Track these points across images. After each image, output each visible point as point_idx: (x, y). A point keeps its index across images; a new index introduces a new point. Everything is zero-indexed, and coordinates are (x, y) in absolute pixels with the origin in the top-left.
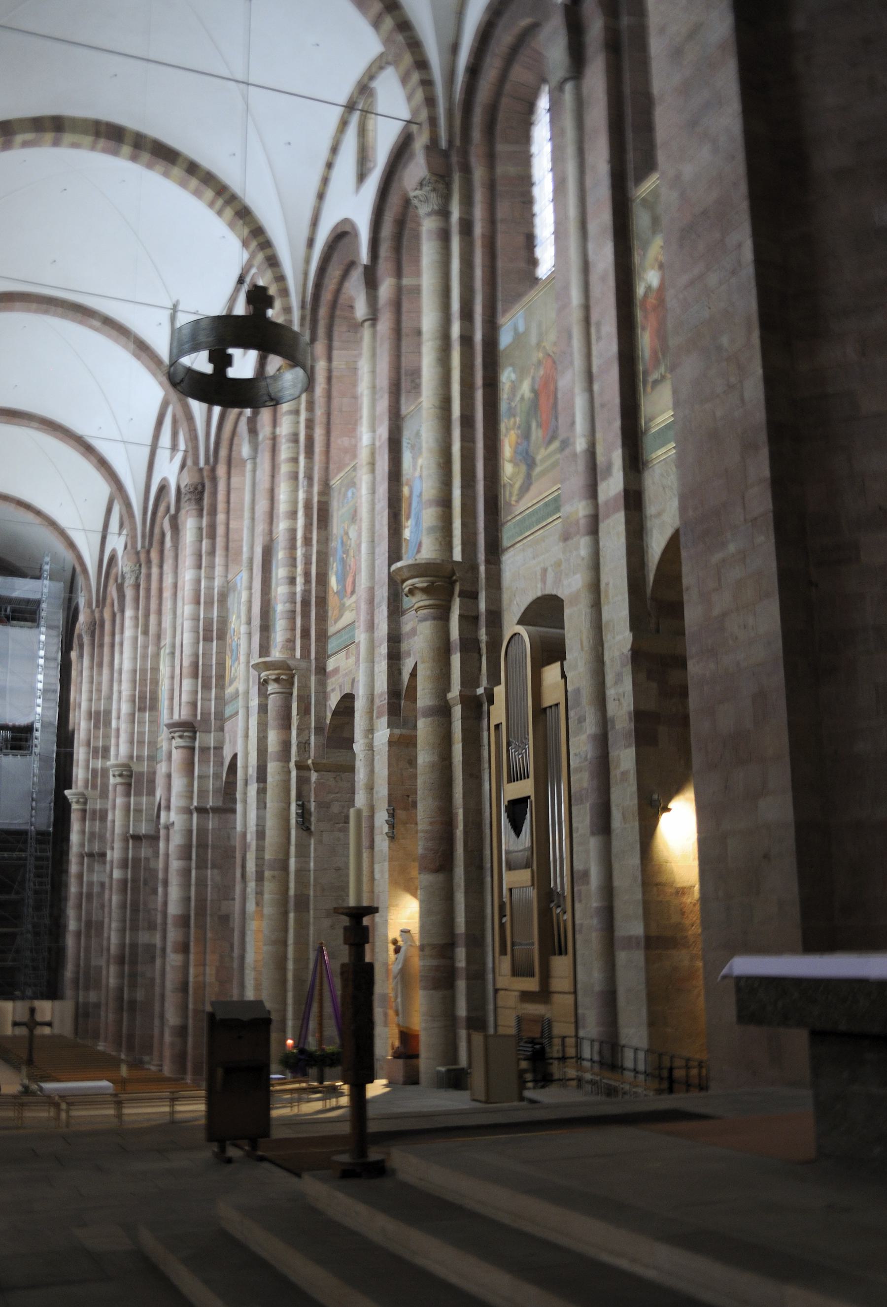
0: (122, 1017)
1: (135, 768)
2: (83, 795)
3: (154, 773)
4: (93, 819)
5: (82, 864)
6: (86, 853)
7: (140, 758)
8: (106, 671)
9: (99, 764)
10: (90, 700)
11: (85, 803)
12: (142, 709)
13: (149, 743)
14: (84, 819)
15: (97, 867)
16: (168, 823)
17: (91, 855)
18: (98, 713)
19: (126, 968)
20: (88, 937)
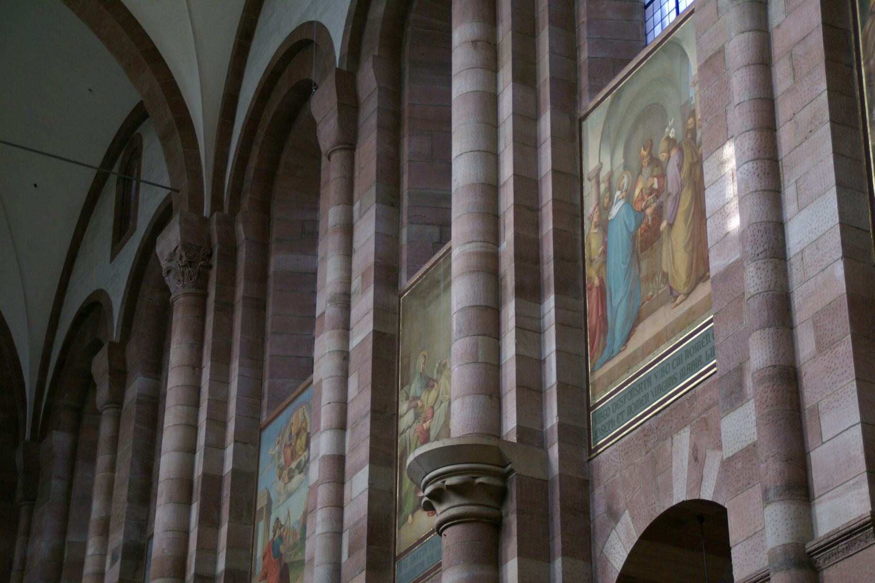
10: (190, 449)
16: (810, 546)
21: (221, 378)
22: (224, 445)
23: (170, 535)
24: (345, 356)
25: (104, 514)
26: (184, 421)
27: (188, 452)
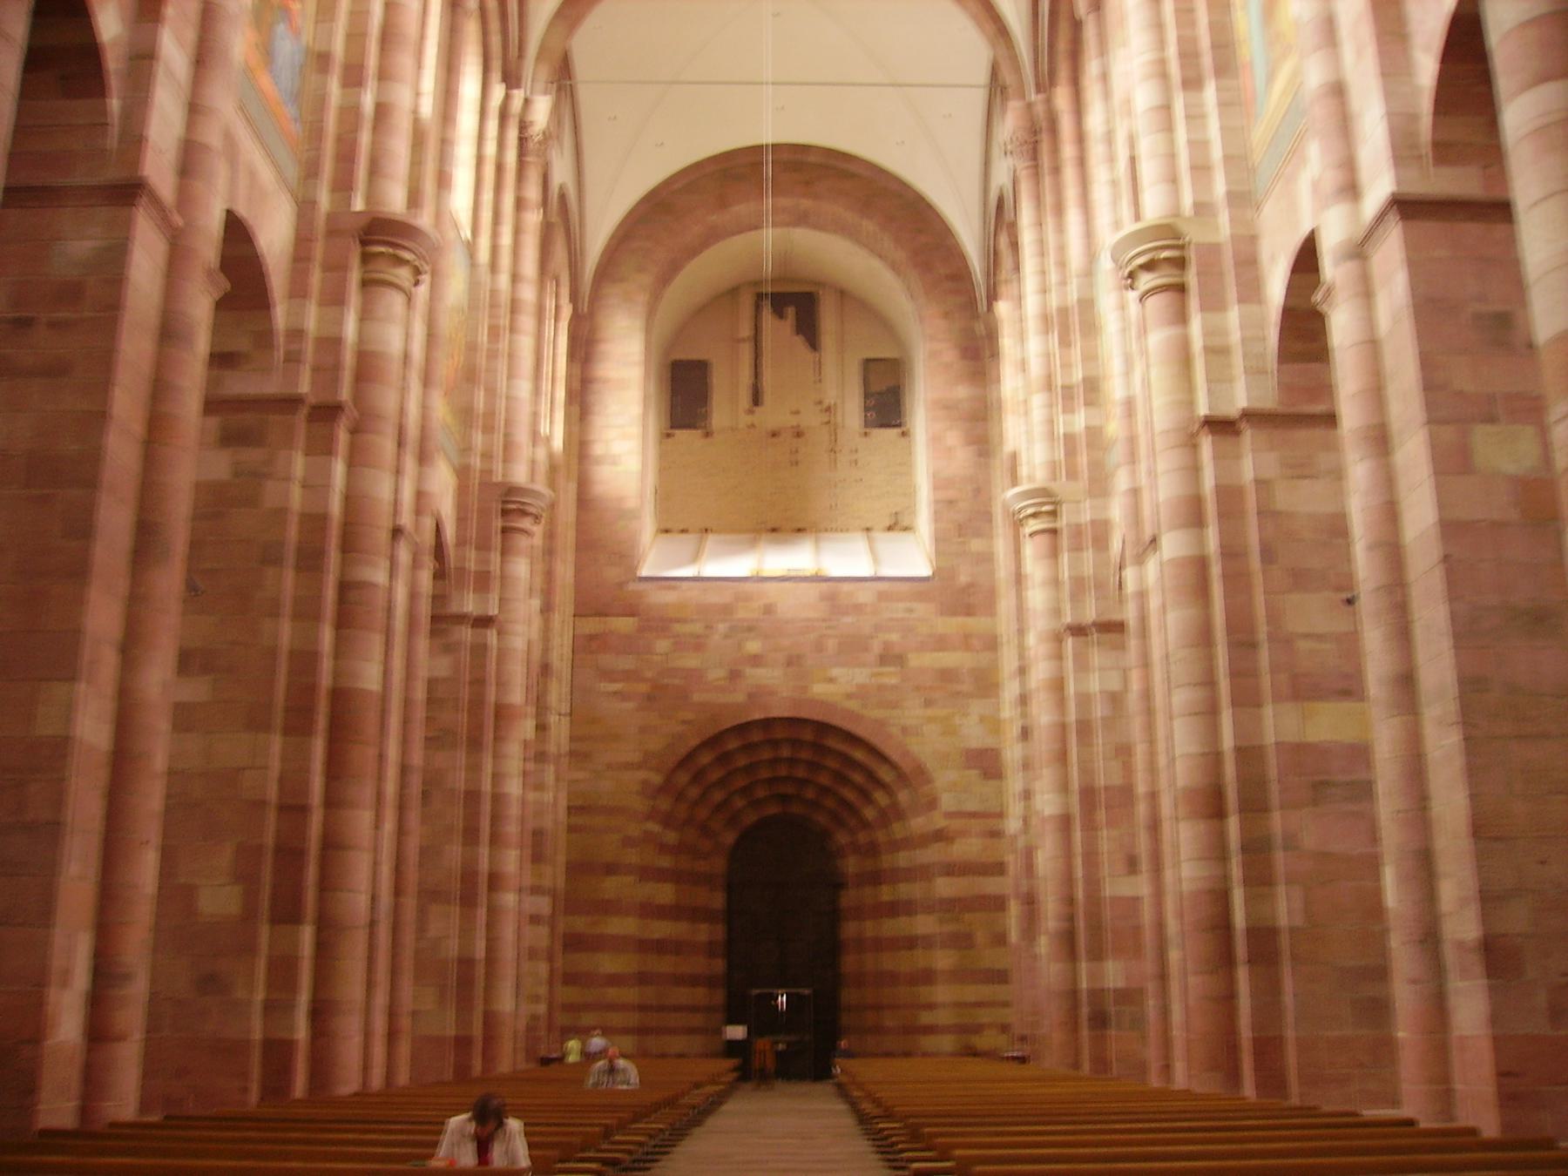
0: (1231, 982)
1: (1194, 235)
2: (1044, 492)
3: (1253, 239)
4: (1077, 548)
5: (1059, 656)
7: (1203, 208)
8: (1073, 217)
9: (1080, 420)
10: (1044, 291)
11: (1054, 514)
12: (1192, 83)
13: (1227, 159)
14: (1054, 553)
15: (1096, 657)
17: (1078, 631)
18: (1064, 312)
19: (1233, 824)
20: (1090, 826)
21: (1060, 228)
24: (1114, 183)
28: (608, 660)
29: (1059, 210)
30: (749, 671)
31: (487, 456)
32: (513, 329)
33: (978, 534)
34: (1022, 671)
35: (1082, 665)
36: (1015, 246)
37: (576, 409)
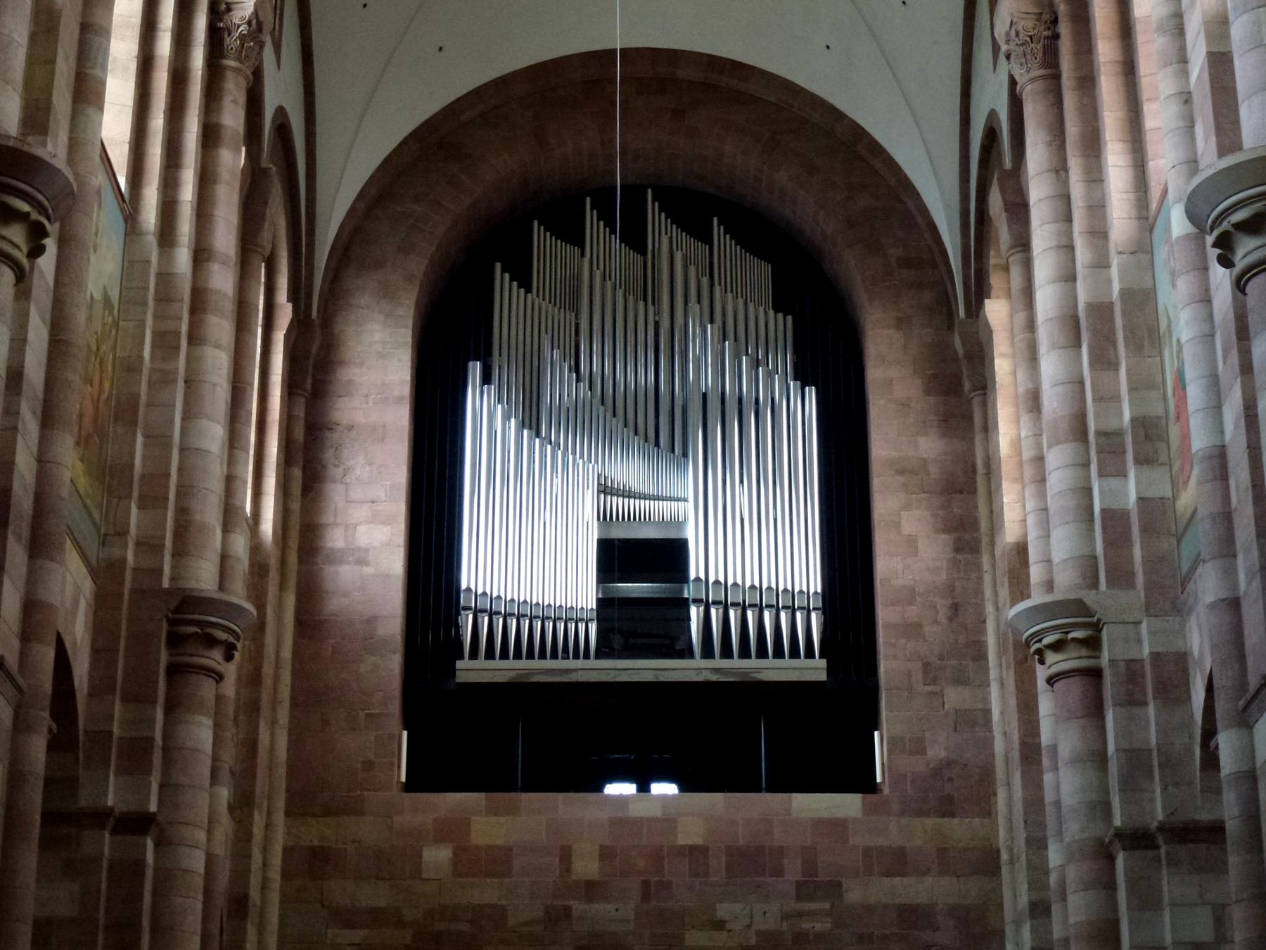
2: (1078, 607)
4: (1132, 700)
6: (1119, 834)
10: (1069, 277)
11: (1093, 643)
14: (1095, 710)
15: (1169, 884)
17: (1137, 839)
21: (1095, 176)
22: (1108, 262)
23: (1060, 389)
25: (1030, 386)
26: (1054, 243)
27: (1065, 281)
28: (341, 891)
29: (1093, 145)
30: (578, 907)
31: (149, 545)
32: (195, 338)
33: (960, 680)
34: (1040, 909)
35: (1147, 900)
36: (1019, 210)
37: (297, 473)
